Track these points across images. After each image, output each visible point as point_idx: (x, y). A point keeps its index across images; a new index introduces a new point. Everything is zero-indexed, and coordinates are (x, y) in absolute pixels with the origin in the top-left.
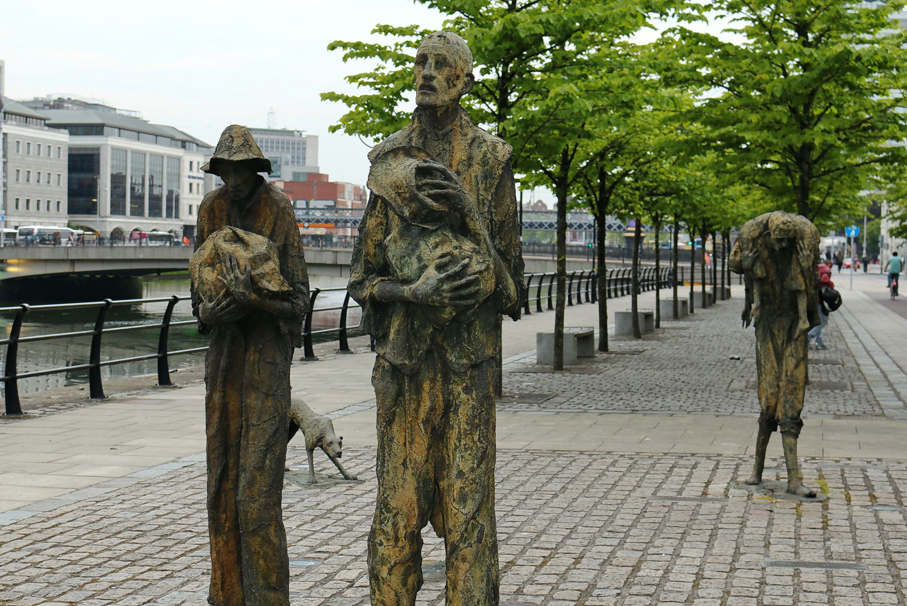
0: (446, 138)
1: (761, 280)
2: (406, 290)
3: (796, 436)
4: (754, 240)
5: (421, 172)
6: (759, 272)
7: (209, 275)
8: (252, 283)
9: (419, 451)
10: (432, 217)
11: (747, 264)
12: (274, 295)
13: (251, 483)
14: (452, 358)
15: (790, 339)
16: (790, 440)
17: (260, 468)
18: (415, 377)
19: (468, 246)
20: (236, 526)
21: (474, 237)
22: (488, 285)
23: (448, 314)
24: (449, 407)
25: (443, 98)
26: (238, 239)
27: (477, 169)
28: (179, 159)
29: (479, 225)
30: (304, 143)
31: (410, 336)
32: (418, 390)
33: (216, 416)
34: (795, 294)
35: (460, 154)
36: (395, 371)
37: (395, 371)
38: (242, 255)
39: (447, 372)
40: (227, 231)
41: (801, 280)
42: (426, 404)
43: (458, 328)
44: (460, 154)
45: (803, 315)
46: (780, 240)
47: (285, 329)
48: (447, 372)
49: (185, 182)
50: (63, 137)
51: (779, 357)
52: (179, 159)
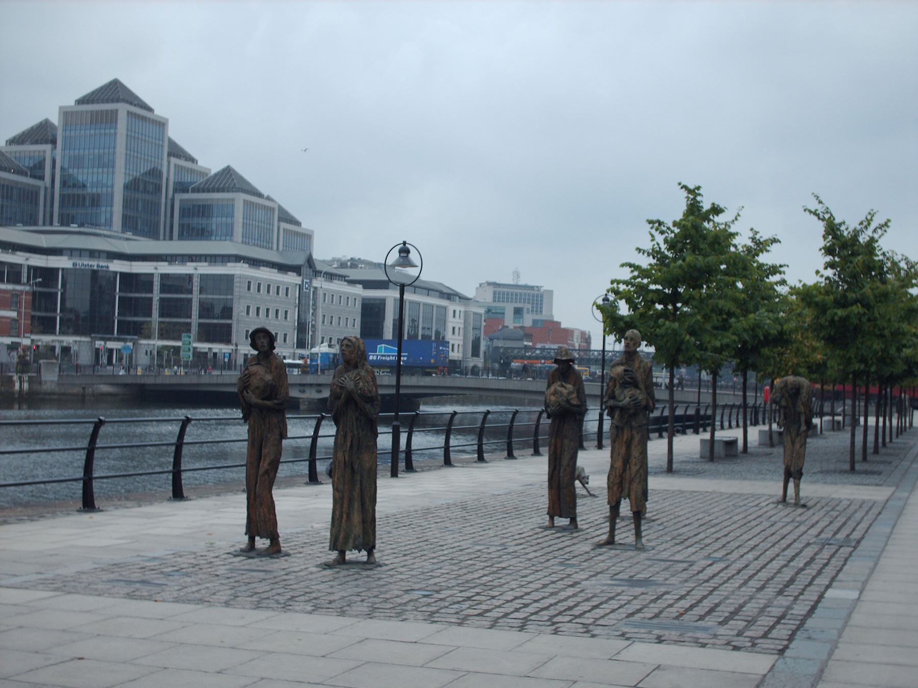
0: (633, 360)
1: (785, 408)
2: (620, 404)
3: (800, 479)
4: (781, 389)
5: (625, 371)
6: (783, 403)
7: (553, 398)
8: (568, 401)
9: (623, 451)
10: (629, 383)
11: (778, 399)
12: (574, 406)
13: (565, 470)
14: (633, 423)
15: (798, 434)
16: (797, 481)
17: (568, 465)
18: (622, 429)
19: (638, 391)
20: (559, 486)
21: (640, 389)
22: (644, 403)
23: (632, 411)
24: (632, 438)
25: (632, 349)
26: (562, 386)
27: (642, 370)
28: (445, 308)
29: (642, 386)
30: (542, 296)
31: (621, 417)
32: (623, 433)
33: (552, 448)
34: (800, 413)
35: (637, 365)
36: (617, 427)
37: (617, 427)
38: (565, 391)
39: (631, 428)
40: (559, 383)
41: (802, 408)
42: (625, 437)
43: (635, 415)
44: (637, 365)
45: (803, 424)
46: (792, 389)
47: (578, 417)
48: (631, 428)
49: (450, 326)
50: (358, 290)
51: (793, 443)
52: (445, 308)
